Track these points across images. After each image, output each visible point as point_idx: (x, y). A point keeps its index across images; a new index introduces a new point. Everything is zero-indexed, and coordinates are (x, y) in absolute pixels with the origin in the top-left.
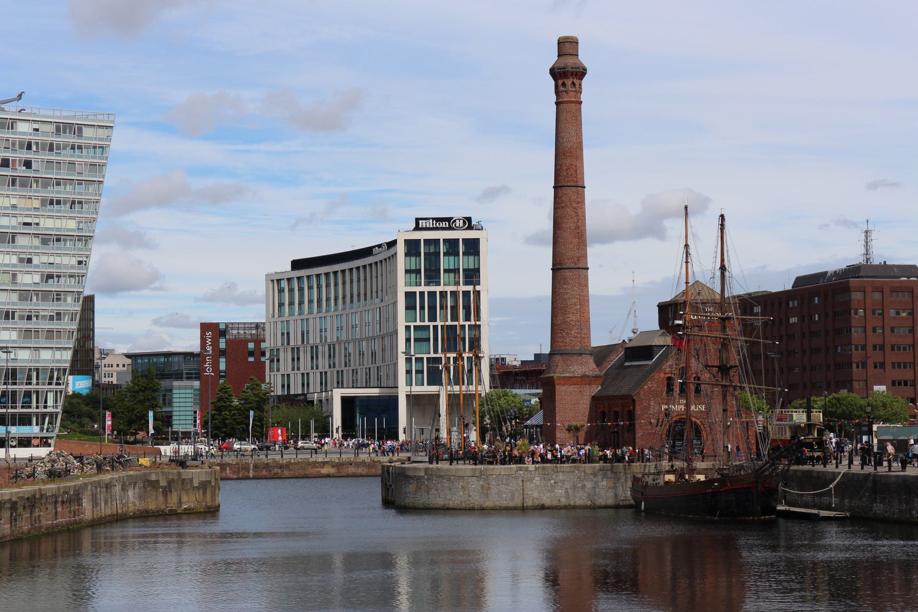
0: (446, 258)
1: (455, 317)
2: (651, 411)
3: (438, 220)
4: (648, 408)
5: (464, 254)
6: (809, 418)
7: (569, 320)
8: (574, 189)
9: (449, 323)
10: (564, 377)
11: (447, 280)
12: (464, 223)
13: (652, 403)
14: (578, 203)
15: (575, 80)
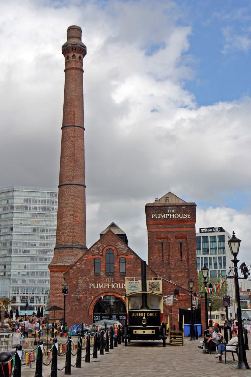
0: (212, 243)
1: (216, 267)
2: (80, 289)
3: (208, 229)
4: (77, 286)
5: (219, 242)
6: (144, 287)
7: (64, 222)
8: (72, 128)
9: (213, 270)
10: (56, 266)
11: (212, 253)
12: (219, 230)
13: (80, 281)
14: (74, 137)
15: (75, 54)
